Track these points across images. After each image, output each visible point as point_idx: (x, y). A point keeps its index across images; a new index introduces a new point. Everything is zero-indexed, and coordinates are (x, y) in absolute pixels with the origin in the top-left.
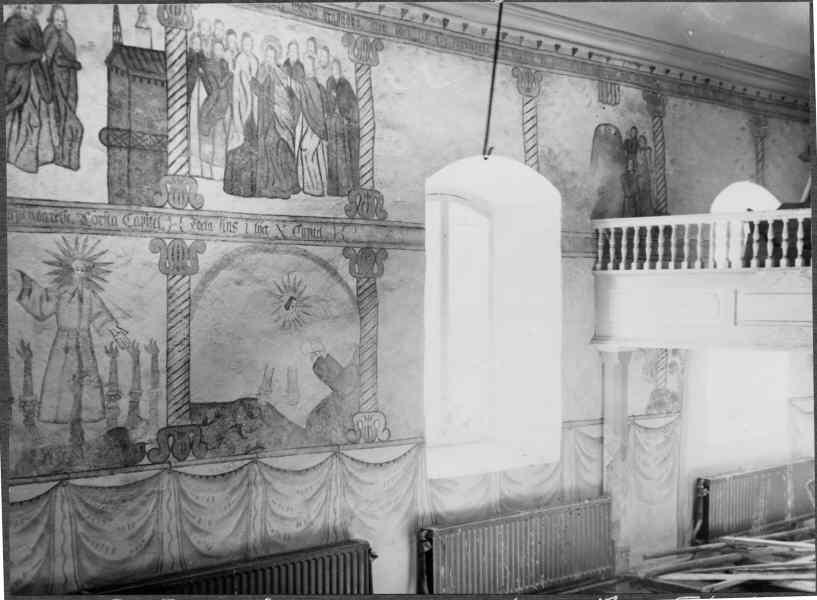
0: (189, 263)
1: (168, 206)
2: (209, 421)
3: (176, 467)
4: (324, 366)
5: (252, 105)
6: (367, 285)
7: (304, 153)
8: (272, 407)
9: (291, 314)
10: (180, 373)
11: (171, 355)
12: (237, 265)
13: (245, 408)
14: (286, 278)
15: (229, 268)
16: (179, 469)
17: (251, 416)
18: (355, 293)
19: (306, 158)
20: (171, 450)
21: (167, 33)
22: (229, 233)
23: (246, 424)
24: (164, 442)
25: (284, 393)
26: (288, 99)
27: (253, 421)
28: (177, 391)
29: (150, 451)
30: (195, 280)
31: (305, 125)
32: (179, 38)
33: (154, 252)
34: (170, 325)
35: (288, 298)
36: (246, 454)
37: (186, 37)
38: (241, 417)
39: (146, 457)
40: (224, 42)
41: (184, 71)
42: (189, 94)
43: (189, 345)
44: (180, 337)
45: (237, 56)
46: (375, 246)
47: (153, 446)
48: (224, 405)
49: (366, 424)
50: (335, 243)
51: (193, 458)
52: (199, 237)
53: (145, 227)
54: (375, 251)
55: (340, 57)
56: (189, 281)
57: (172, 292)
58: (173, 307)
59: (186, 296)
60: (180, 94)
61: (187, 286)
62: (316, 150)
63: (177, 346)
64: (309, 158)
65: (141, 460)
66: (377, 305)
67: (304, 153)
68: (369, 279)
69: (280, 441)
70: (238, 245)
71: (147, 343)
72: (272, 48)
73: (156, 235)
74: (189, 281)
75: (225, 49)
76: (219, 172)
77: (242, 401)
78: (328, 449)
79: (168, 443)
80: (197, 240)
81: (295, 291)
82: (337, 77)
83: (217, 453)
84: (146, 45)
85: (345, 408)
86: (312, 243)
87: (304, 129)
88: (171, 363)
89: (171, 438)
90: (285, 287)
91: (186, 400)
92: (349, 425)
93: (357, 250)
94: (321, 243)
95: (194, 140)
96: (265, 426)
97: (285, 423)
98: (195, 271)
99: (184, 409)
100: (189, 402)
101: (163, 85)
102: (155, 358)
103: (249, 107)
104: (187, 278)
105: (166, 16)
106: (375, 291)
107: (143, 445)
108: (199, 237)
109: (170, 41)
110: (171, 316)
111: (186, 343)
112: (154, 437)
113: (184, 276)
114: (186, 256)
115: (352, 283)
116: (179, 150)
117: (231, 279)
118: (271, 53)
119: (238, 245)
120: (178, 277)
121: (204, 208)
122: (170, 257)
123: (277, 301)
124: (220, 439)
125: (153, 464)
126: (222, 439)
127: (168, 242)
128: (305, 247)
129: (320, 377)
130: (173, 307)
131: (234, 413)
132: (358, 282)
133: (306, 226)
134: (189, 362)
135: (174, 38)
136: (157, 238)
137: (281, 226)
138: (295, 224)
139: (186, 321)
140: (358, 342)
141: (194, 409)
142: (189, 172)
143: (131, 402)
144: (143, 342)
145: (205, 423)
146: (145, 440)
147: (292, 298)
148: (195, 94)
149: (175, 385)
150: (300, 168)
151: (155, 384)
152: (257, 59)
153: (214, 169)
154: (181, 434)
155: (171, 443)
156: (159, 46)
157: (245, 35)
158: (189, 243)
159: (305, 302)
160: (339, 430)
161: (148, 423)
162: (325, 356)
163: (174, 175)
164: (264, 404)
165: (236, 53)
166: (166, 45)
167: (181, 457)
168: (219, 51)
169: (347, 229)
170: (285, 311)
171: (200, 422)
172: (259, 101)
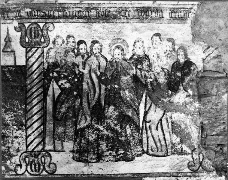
1: (26, 173)
5: (100, 94)
7: (148, 124)
19: (150, 127)
21: (27, 53)
26: (132, 85)
31: (149, 102)
32: (36, 55)
37: (43, 53)
40: (76, 51)
41: (41, 77)
42: (45, 93)
45: (86, 60)
55: (186, 44)
60: (36, 94)
62: (161, 120)
64: (153, 127)
67: (148, 124)
72: (117, 47)
75: (76, 56)
76: (69, 145)
82: (182, 61)
84: (11, 63)
87: (147, 108)
95: (50, 126)
101: (22, 89)
103: (97, 95)
105: (27, 40)
109: (30, 57)
116: (36, 133)
118: (118, 51)
121: (56, 173)
135: (33, 55)
142: (43, 148)
148: (50, 92)
150: (144, 136)
152: (106, 59)
153: (65, 144)
156: (21, 62)
157: (94, 42)
163: (33, 151)
165: (86, 56)
166: (27, 60)
168: (71, 59)
172: (106, 89)
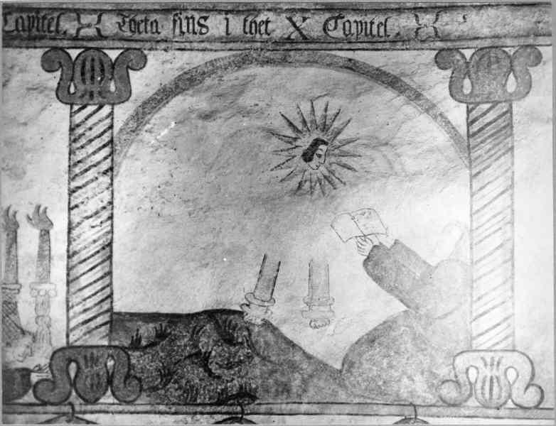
0: (112, 87)
2: (144, 343)
3: (81, 412)
4: (387, 263)
6: (490, 117)
8: (274, 330)
9: (316, 169)
10: (97, 259)
11: (75, 233)
12: (209, 88)
13: (217, 327)
14: (305, 108)
15: (190, 92)
16: (88, 417)
17: (230, 341)
18: (463, 130)
20: (73, 384)
22: (191, 37)
23: (217, 352)
24: (61, 370)
25: (303, 306)
27: (233, 349)
28: (87, 292)
29: (38, 383)
30: (123, 113)
33: (50, 70)
34: (74, 184)
35: (311, 140)
36: (219, 404)
38: (207, 340)
39: (31, 391)
43: (111, 218)
44: (92, 207)
46: (509, 42)
47: (44, 376)
48: (174, 318)
49: (488, 373)
50: (419, 45)
51: (112, 400)
52: (134, 45)
53: (34, 32)
54: (511, 51)
56: (111, 114)
57: (80, 131)
58: (80, 155)
59: (106, 138)
61: (108, 121)
63: (87, 218)
65: (20, 396)
66: (512, 149)
68: (495, 103)
69: (286, 389)
70: (210, 56)
71: (31, 212)
73: (54, 43)
74: (111, 114)
77: (211, 314)
78: (394, 410)
79: (68, 374)
80: (128, 49)
81: (325, 128)
83: (159, 396)
85: (435, 340)
86: (364, 46)
88: (75, 246)
89: (73, 365)
90: (304, 122)
91: (106, 306)
92: (443, 372)
93: (468, 53)
94: (387, 45)
96: (257, 359)
97: (298, 357)
98: (125, 94)
99: (100, 320)
100: (110, 310)
102: (45, 234)
104: (106, 110)
106: (510, 125)
107: (26, 373)
108: (134, 45)
110: (77, 170)
111: (105, 214)
112: (44, 361)
113: (101, 107)
114: (108, 75)
115: (457, 114)
117: (192, 111)
119: (210, 56)
120: (90, 109)
122: (78, 74)
123: (285, 146)
124: (167, 375)
125: (44, 404)
126: (171, 374)
127: (74, 53)
128: (350, 54)
129: (378, 279)
130: (80, 155)
131: (195, 332)
132: (469, 112)
133: (352, 17)
134: (110, 244)
136: (55, 48)
137: (297, 18)
138: (327, 15)
139: (106, 179)
140: (467, 220)
141: (117, 321)
143: (5, 302)
144: (23, 211)
145: (136, 344)
146: (30, 364)
147: (317, 143)
149: (84, 281)
151: (44, 277)
154: (94, 360)
155: (72, 375)
158: (113, 55)
159: (346, 148)
160: (418, 378)
161: (34, 338)
162: (388, 243)
164: (259, 322)
167: (90, 396)
169: (445, 17)
170: (303, 163)
171: (127, 343)
